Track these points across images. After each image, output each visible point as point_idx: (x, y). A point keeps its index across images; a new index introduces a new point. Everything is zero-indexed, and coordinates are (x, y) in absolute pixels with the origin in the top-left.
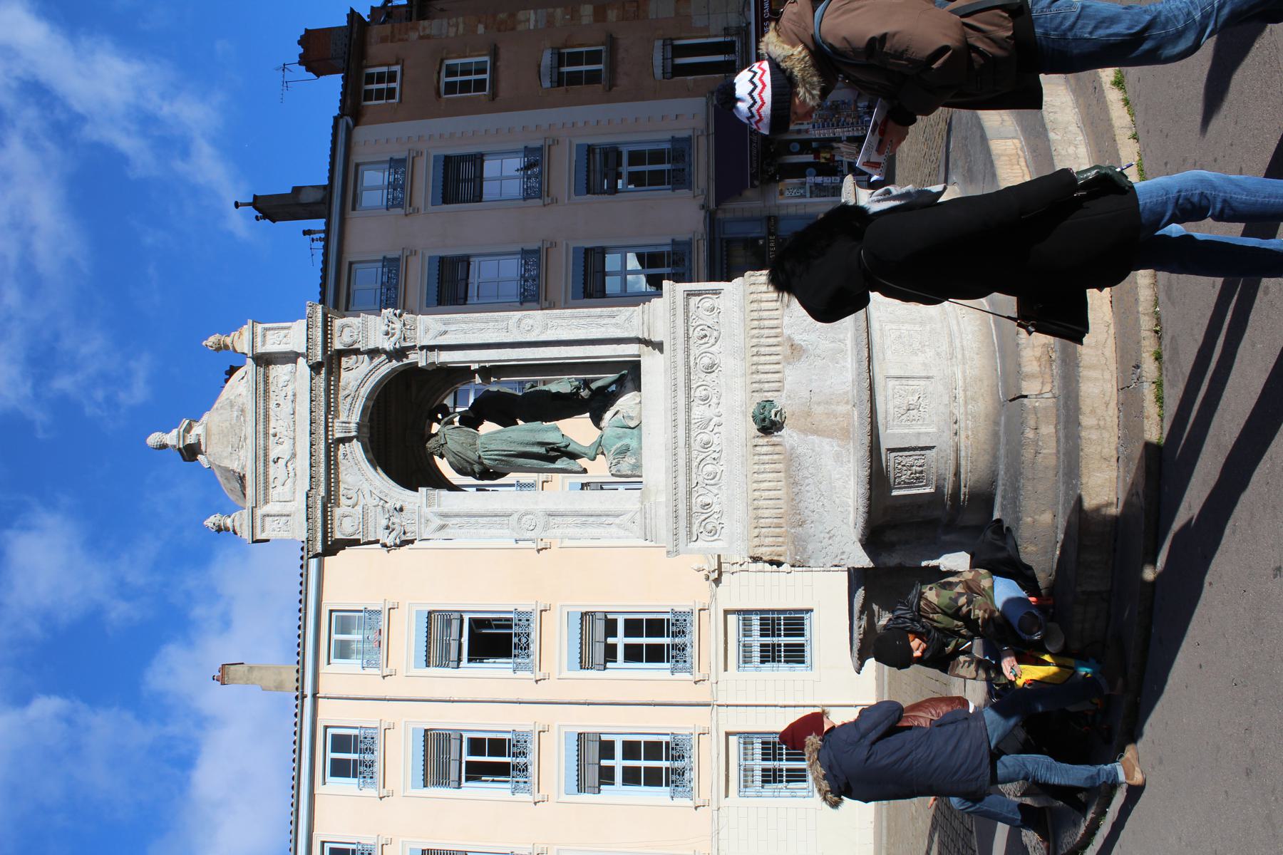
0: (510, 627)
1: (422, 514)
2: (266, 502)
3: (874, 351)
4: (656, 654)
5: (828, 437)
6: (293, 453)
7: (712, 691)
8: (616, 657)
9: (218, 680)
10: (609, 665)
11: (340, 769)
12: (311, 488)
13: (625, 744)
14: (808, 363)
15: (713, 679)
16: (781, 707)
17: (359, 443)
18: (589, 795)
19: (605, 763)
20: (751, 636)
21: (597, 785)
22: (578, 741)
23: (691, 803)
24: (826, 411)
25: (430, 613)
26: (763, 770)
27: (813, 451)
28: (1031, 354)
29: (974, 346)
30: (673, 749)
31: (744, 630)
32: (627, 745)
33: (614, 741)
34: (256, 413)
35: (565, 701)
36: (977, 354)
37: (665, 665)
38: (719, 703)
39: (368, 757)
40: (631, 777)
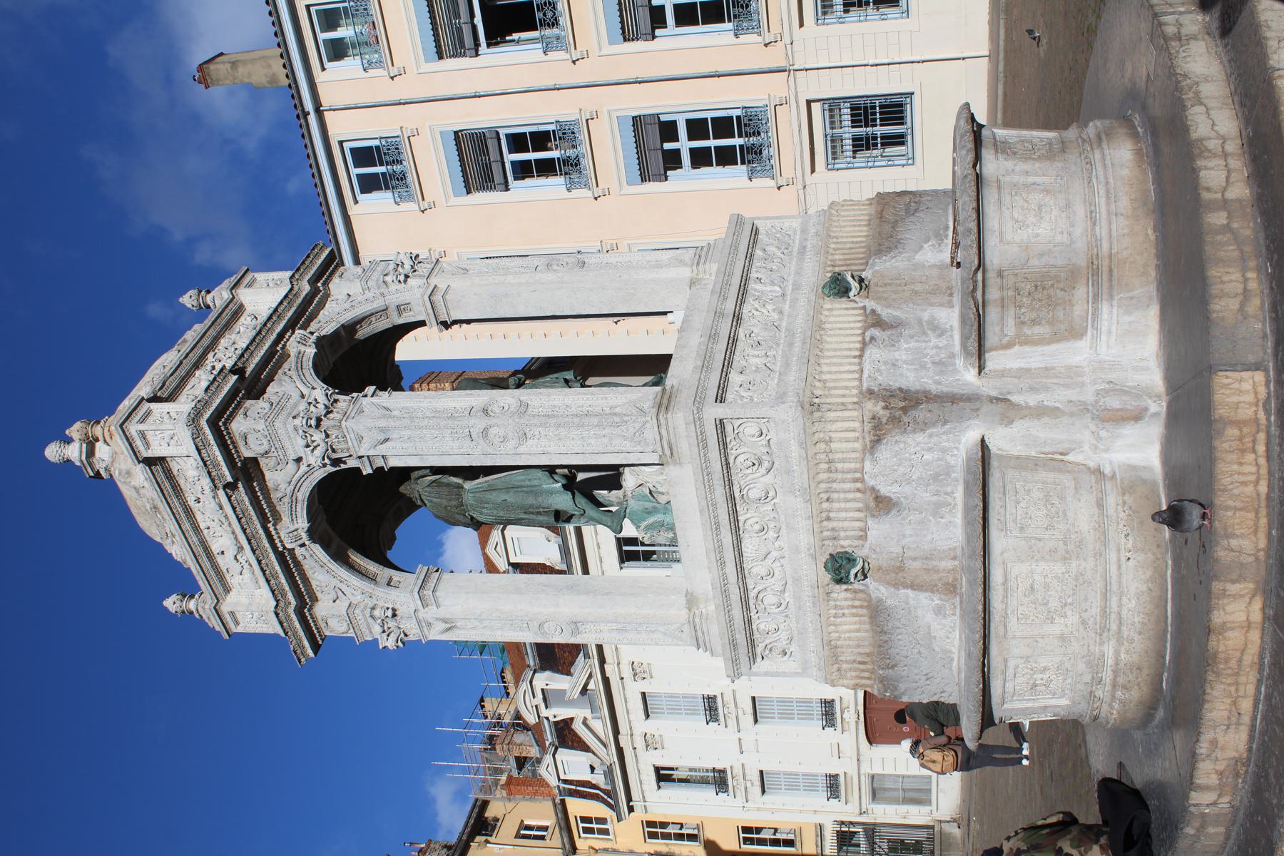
1: (421, 618)
2: (227, 590)
3: (992, 628)
5: (926, 591)
7: (787, 54)
8: (665, 22)
9: (200, 83)
10: (658, 32)
11: (369, 184)
12: (277, 601)
13: (689, 122)
14: (900, 518)
15: (787, 40)
16: (872, 66)
18: (656, 183)
19: (668, 146)
21: (662, 172)
22: (633, 125)
23: (772, 183)
24: (925, 567)
26: (854, 140)
27: (907, 603)
28: (1211, 766)
29: (1137, 620)
30: (745, 125)
33: (675, 121)
35: (611, 82)
36: (1140, 633)
37: (728, 26)
39: (397, 168)
40: (700, 159)
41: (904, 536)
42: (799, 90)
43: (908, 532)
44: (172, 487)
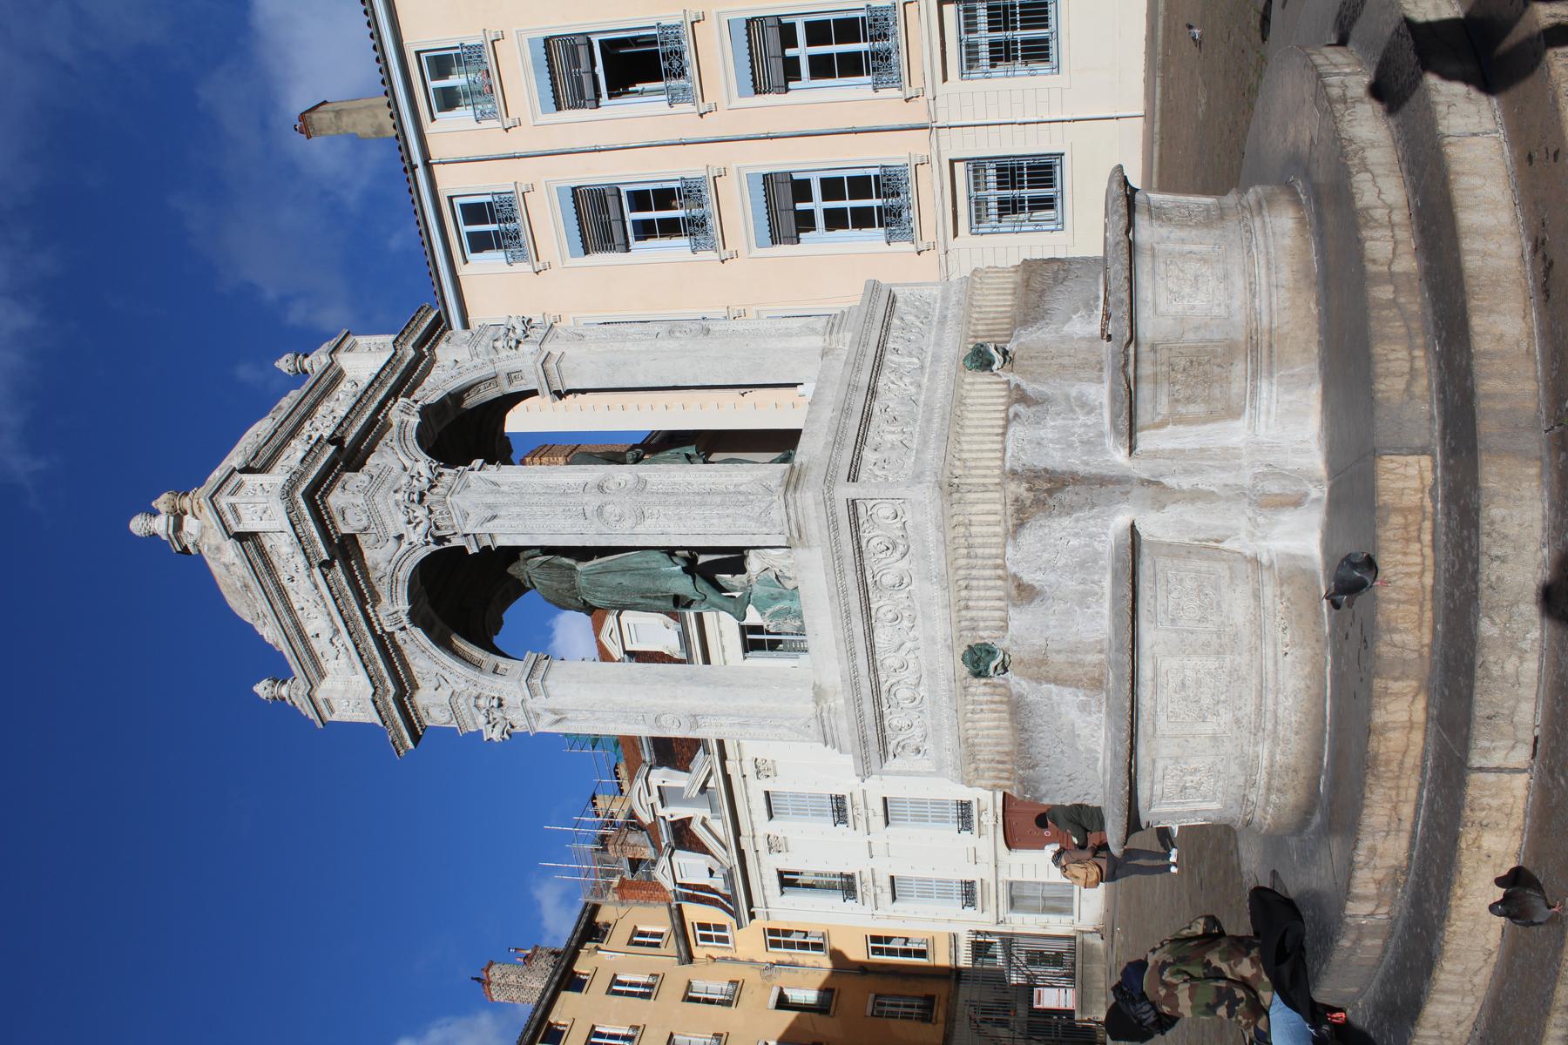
0: (655, 43)
2: (322, 676)
3: (1140, 726)
4: (851, 66)
5: (1070, 686)
6: (335, 630)
7: (929, 111)
10: (791, 85)
11: (480, 243)
12: (375, 688)
13: (824, 182)
15: (929, 95)
17: (419, 629)
19: (800, 206)
20: (976, 31)
21: (794, 234)
22: (764, 184)
23: (912, 247)
24: (1070, 660)
25: (547, 40)
26: (1000, 203)
27: (1050, 699)
28: (1369, 875)
29: (1293, 719)
31: (967, 25)
32: (825, 182)
34: (265, 593)
36: (1297, 733)
38: (938, 124)
39: (511, 226)
40: (835, 220)
41: (1048, 627)
42: (942, 148)
43: (1052, 623)
44: (265, 565)
